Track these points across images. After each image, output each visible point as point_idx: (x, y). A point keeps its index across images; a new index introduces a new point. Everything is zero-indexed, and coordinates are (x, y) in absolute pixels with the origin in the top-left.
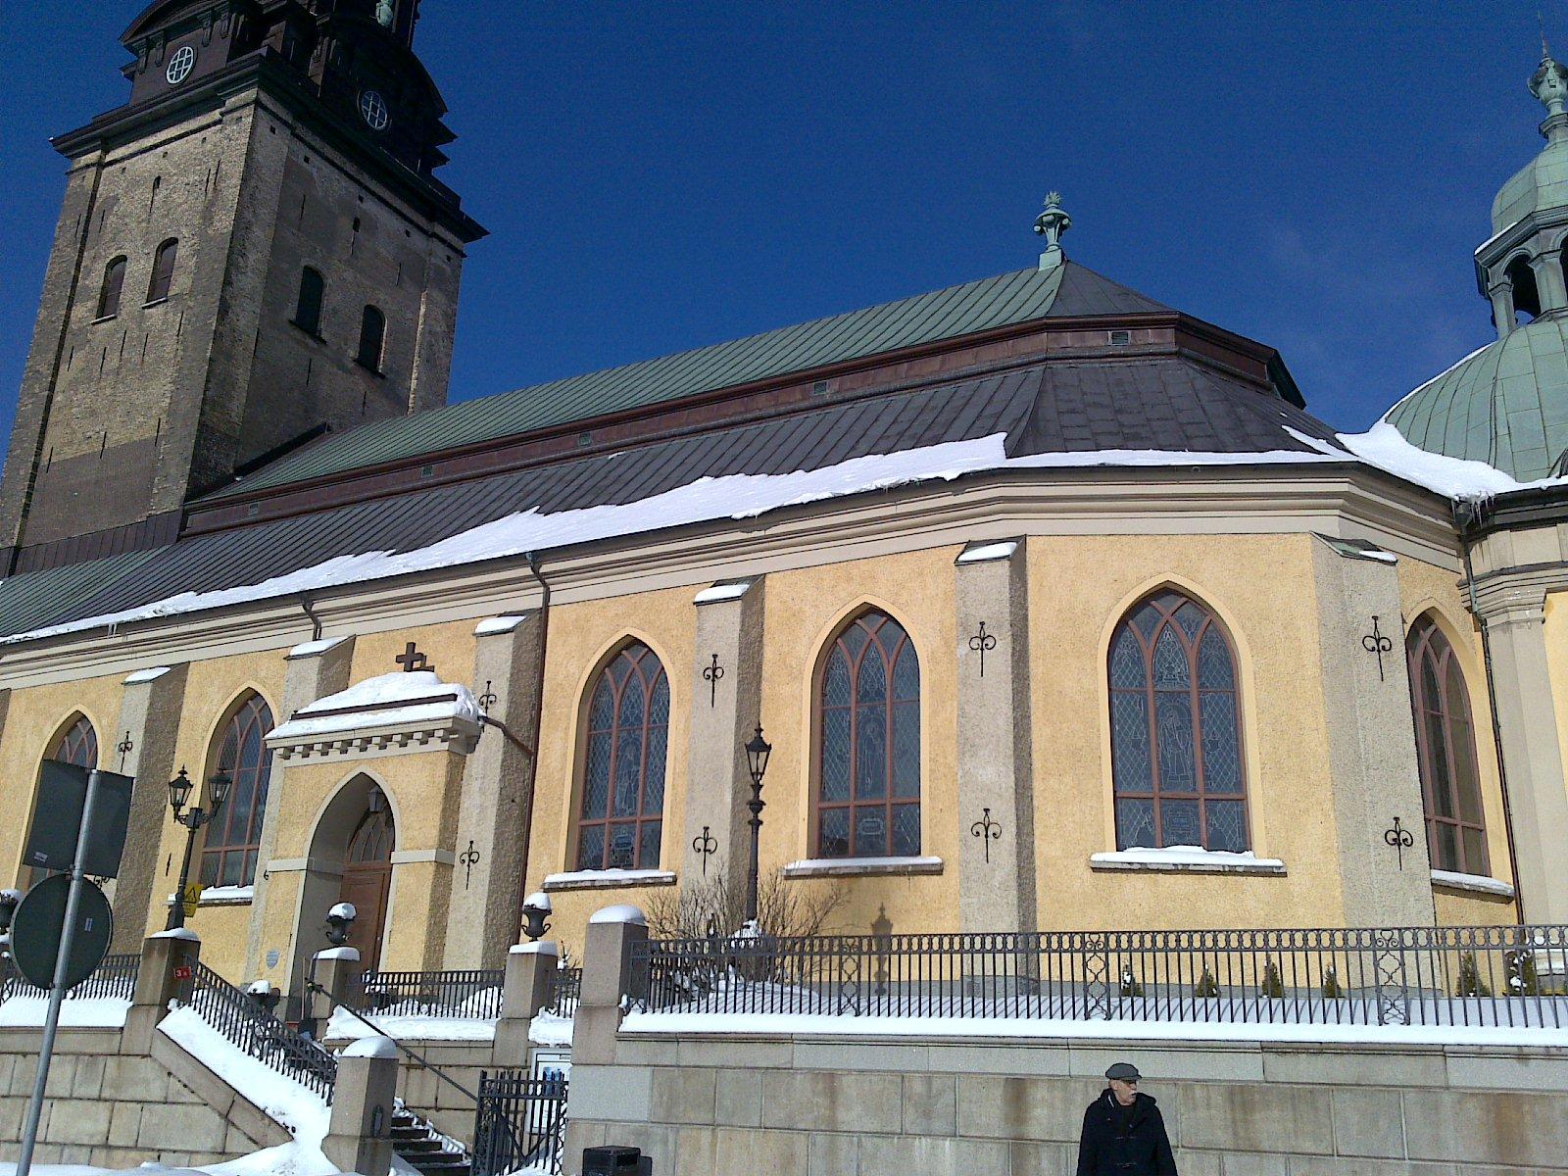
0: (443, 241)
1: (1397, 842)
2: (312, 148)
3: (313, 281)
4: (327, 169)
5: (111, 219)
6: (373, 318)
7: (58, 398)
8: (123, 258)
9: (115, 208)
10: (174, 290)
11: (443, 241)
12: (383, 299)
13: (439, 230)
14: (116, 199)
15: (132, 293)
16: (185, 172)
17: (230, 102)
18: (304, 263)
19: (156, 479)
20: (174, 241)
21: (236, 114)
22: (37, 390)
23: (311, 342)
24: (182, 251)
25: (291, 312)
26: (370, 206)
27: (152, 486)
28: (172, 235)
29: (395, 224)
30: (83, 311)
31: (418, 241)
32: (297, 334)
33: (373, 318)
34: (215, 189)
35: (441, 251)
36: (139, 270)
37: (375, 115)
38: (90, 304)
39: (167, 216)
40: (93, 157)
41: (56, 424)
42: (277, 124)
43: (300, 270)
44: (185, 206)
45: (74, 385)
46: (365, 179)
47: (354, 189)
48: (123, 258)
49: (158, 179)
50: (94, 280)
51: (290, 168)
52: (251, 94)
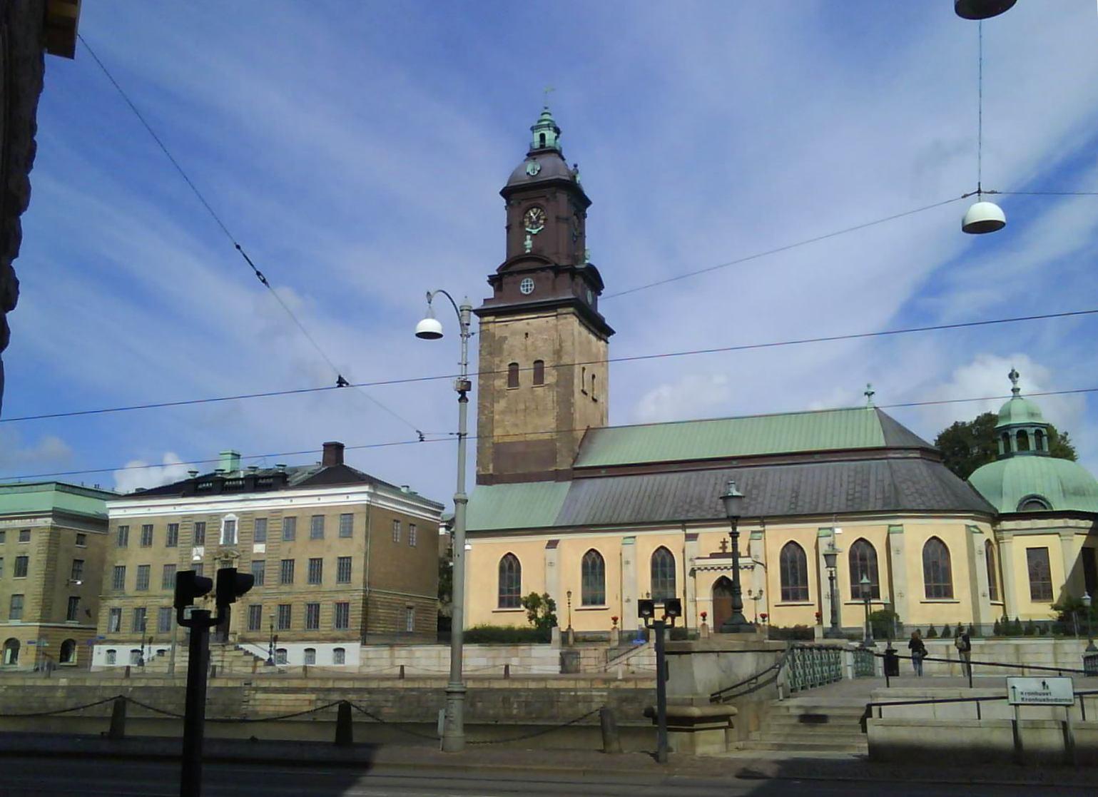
1: (984, 596)
5: (505, 346)
7: (497, 417)
9: (506, 342)
10: (546, 382)
14: (506, 338)
16: (540, 333)
17: (560, 310)
19: (558, 456)
21: (564, 316)
22: (486, 412)
23: (585, 396)
27: (556, 459)
28: (539, 359)
30: (501, 383)
34: (560, 345)
38: (504, 380)
39: (534, 350)
40: (491, 319)
41: (498, 427)
44: (543, 348)
45: (503, 413)
46: (591, 327)
48: (516, 364)
49: (527, 334)
52: (571, 309)
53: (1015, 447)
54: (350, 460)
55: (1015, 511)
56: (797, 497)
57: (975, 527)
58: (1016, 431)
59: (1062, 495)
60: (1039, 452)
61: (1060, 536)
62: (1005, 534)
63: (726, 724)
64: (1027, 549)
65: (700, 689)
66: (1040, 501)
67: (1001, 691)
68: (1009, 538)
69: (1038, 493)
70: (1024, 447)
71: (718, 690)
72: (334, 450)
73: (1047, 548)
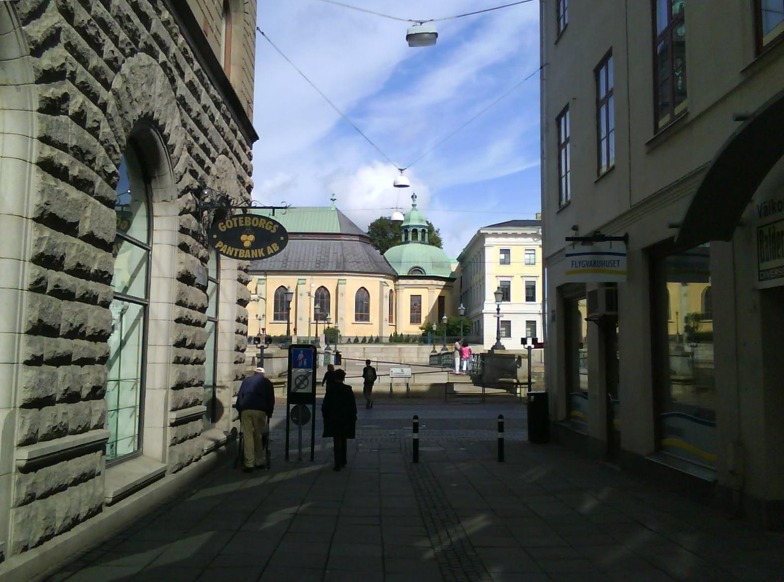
53: (410, 238)
55: (407, 275)
56: (287, 260)
57: (385, 282)
58: (412, 228)
59: (431, 267)
60: (423, 242)
61: (428, 289)
62: (400, 287)
63: (284, 385)
64: (411, 296)
65: (275, 372)
66: (420, 270)
67: (387, 373)
68: (402, 289)
69: (420, 265)
70: (415, 237)
71: (281, 372)
73: (421, 296)
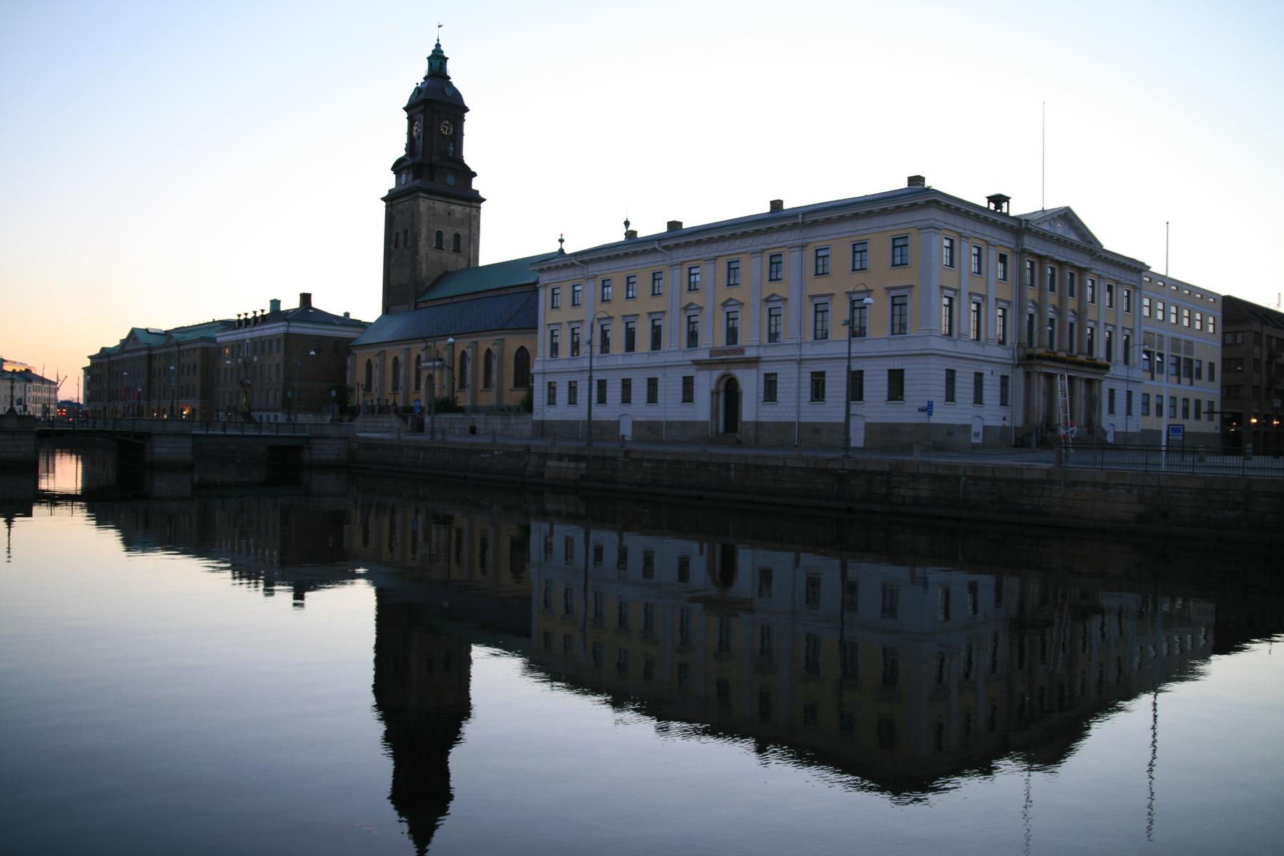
0: (474, 207)
2: (434, 200)
3: (440, 234)
4: (439, 203)
6: (457, 237)
8: (397, 234)
11: (474, 207)
12: (459, 231)
13: (474, 204)
15: (401, 245)
18: (436, 230)
20: (406, 232)
23: (441, 251)
24: (409, 234)
25: (434, 245)
26: (453, 207)
29: (460, 208)
30: (392, 246)
31: (467, 209)
32: (437, 250)
33: (457, 237)
35: (474, 210)
36: (401, 237)
37: (451, 180)
42: (426, 200)
43: (435, 233)
47: (447, 204)
50: (394, 238)
51: (430, 208)
54: (316, 304)
72: (306, 298)
